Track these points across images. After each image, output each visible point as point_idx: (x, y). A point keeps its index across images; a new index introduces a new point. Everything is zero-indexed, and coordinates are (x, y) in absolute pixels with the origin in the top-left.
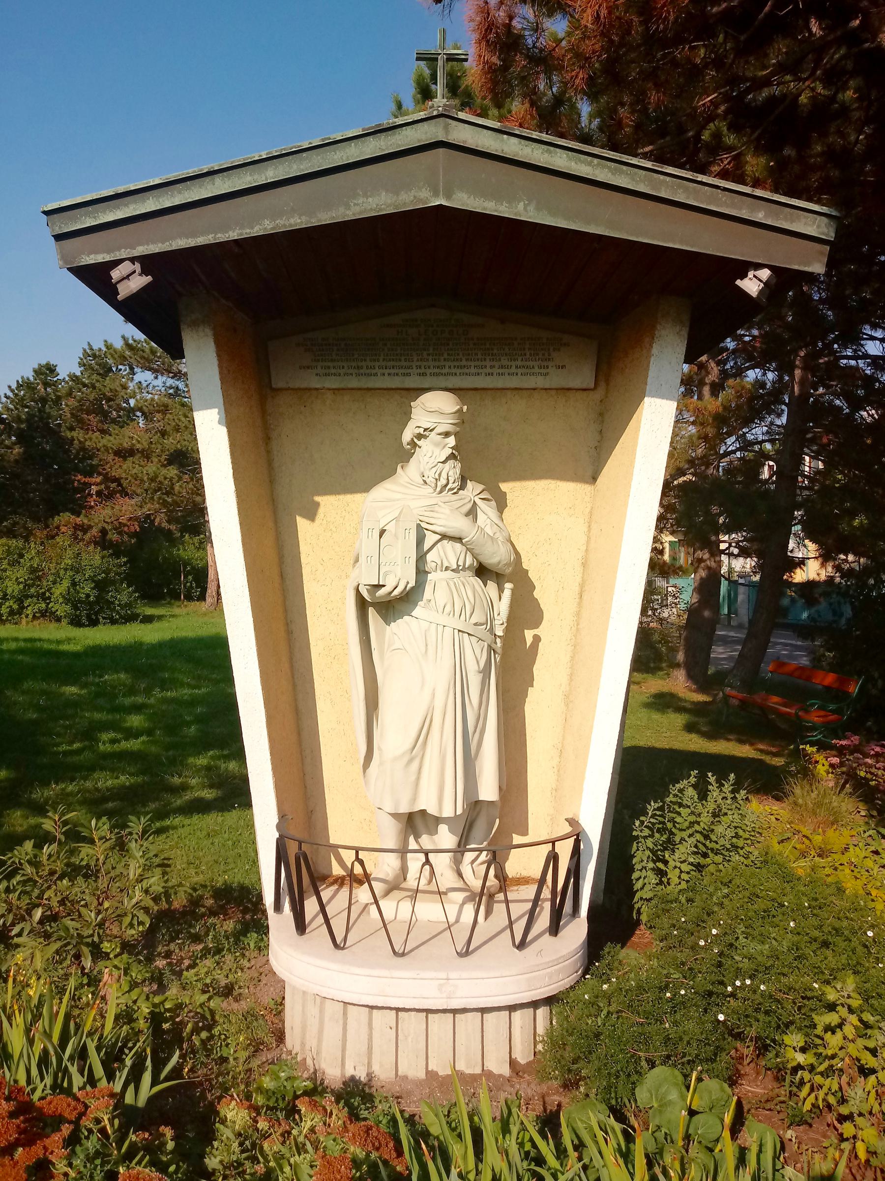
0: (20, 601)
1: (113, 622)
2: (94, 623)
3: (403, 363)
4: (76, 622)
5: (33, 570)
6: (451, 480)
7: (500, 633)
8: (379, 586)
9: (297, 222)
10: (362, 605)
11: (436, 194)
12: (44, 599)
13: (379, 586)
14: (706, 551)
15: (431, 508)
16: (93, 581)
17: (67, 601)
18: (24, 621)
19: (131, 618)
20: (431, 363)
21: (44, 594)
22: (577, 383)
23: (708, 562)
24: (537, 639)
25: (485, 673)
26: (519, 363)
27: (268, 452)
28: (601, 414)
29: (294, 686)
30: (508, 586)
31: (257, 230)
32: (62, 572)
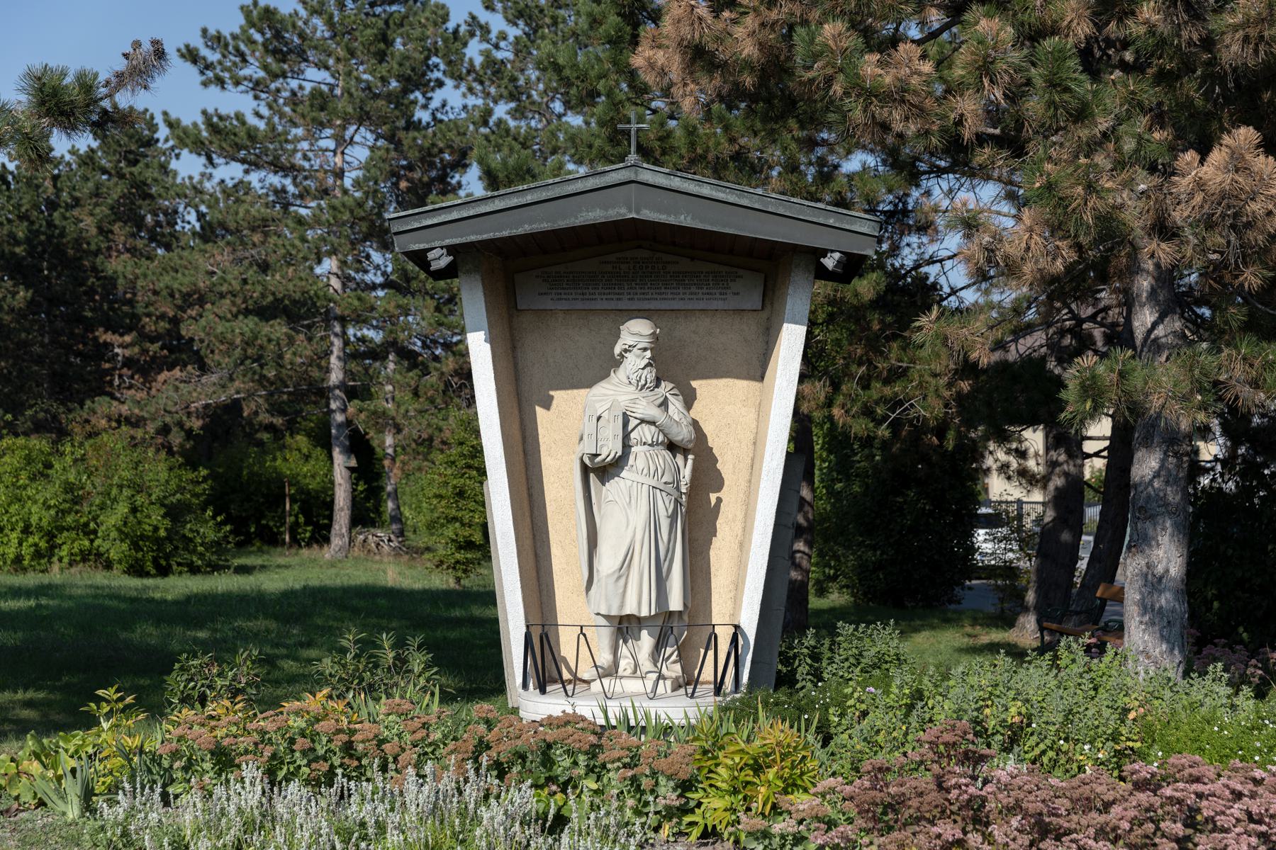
0: (50, 536)
1: (194, 570)
2: (164, 572)
4: (136, 570)
5: (69, 488)
7: (684, 490)
8: (597, 455)
9: (545, 226)
10: (585, 470)
11: (630, 212)
12: (86, 534)
13: (597, 455)
14: (1062, 450)
15: (634, 401)
16: (163, 505)
17: (123, 536)
18: (56, 567)
19: (215, 568)
21: (86, 525)
22: (748, 306)
23: (1065, 467)
24: (719, 500)
25: (673, 518)
27: (514, 358)
28: (768, 329)
29: (534, 536)
30: (691, 457)
31: (520, 231)
32: (114, 491)
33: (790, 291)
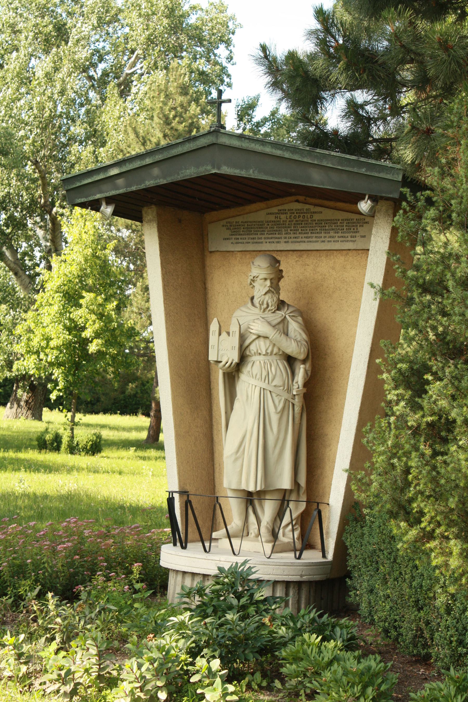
3: (277, 236)
6: (270, 304)
11: (214, 168)
20: (292, 236)
26: (340, 234)
33: (374, 232)
